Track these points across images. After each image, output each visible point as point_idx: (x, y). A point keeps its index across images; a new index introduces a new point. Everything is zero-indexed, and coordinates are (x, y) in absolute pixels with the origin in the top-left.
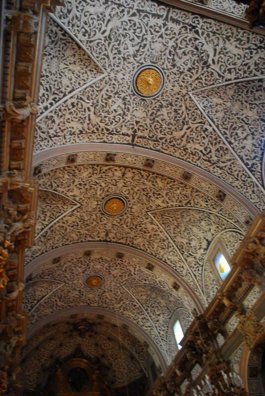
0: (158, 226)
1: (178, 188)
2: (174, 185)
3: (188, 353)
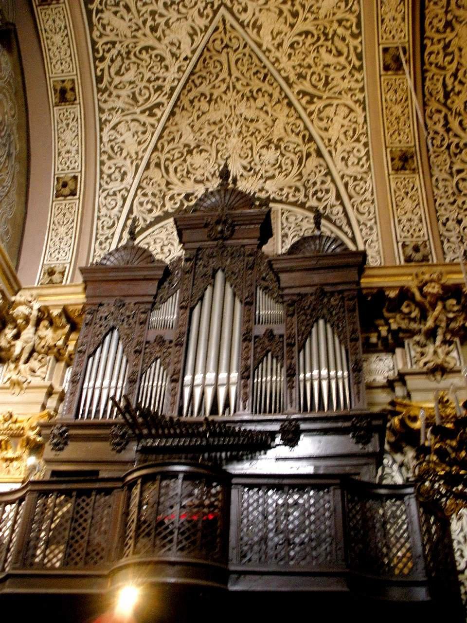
0: (193, 52)
1: (340, 54)
2: (344, 39)
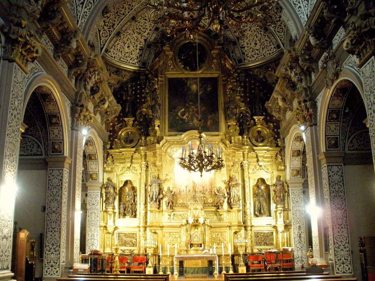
3: (326, 9)
